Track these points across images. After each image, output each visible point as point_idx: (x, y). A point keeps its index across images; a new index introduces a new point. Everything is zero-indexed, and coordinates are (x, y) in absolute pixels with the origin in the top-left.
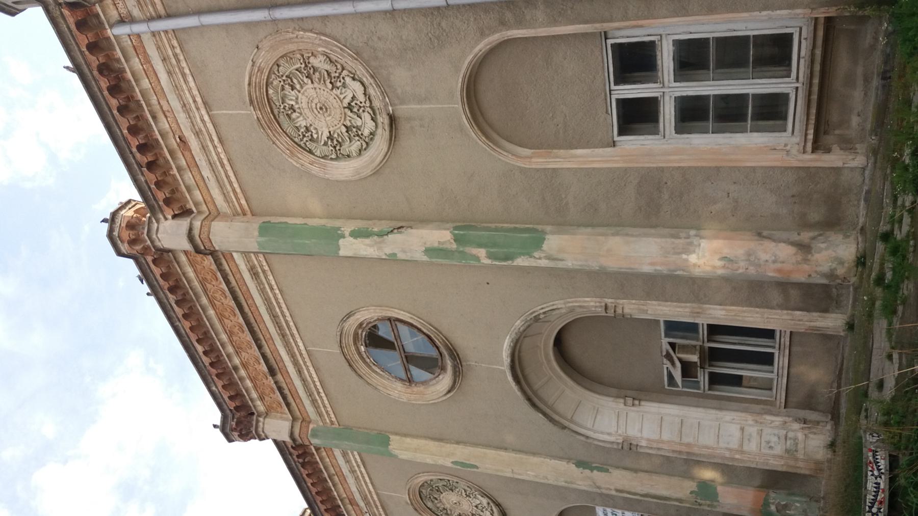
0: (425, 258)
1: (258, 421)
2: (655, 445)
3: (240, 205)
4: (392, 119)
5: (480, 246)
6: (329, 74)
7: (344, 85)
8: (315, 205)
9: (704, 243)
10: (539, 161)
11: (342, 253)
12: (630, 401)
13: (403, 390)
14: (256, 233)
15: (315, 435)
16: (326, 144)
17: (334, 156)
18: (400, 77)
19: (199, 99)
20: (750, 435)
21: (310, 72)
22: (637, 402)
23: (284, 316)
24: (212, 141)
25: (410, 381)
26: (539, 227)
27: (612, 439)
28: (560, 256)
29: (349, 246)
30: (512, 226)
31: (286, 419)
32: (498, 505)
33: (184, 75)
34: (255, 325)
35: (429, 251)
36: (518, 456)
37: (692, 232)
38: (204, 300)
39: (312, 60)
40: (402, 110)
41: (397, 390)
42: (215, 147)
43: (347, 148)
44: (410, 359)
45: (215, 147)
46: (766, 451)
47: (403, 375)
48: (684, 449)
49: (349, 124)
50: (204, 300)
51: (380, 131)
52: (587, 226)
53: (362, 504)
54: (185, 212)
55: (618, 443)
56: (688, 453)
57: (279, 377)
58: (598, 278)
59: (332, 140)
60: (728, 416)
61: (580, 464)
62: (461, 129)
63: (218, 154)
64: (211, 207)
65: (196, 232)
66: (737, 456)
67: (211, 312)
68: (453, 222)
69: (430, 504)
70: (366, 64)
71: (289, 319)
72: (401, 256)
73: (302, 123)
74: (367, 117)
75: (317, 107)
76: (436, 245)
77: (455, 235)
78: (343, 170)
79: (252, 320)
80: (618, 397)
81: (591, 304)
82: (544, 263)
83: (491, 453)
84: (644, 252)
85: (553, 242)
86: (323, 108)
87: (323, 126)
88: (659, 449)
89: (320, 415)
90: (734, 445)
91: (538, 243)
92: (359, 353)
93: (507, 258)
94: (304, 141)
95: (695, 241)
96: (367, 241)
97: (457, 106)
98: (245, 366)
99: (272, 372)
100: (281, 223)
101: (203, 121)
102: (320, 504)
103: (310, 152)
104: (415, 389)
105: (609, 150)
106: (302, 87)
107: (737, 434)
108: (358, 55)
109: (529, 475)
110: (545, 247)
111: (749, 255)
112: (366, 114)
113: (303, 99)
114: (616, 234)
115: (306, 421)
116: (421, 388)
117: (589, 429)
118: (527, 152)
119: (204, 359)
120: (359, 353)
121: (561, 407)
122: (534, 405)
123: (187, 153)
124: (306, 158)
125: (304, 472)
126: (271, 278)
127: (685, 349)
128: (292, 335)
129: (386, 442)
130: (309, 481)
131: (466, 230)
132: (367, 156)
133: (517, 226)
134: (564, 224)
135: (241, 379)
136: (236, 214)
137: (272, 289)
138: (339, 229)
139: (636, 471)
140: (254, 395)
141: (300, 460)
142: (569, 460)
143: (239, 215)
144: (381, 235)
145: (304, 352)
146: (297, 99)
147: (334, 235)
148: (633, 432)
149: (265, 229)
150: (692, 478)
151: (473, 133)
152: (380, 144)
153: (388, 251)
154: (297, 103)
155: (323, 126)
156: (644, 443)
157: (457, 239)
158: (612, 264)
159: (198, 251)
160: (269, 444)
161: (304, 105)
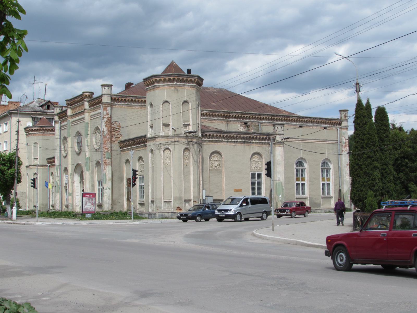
26: (90, 170)
46: (76, 203)
54: (90, 107)
57: (75, 115)
61: (71, 173)
85: (87, 173)
90: (76, 198)
99: (76, 114)
114: (89, 181)
148: (76, 182)
157: (87, 158)
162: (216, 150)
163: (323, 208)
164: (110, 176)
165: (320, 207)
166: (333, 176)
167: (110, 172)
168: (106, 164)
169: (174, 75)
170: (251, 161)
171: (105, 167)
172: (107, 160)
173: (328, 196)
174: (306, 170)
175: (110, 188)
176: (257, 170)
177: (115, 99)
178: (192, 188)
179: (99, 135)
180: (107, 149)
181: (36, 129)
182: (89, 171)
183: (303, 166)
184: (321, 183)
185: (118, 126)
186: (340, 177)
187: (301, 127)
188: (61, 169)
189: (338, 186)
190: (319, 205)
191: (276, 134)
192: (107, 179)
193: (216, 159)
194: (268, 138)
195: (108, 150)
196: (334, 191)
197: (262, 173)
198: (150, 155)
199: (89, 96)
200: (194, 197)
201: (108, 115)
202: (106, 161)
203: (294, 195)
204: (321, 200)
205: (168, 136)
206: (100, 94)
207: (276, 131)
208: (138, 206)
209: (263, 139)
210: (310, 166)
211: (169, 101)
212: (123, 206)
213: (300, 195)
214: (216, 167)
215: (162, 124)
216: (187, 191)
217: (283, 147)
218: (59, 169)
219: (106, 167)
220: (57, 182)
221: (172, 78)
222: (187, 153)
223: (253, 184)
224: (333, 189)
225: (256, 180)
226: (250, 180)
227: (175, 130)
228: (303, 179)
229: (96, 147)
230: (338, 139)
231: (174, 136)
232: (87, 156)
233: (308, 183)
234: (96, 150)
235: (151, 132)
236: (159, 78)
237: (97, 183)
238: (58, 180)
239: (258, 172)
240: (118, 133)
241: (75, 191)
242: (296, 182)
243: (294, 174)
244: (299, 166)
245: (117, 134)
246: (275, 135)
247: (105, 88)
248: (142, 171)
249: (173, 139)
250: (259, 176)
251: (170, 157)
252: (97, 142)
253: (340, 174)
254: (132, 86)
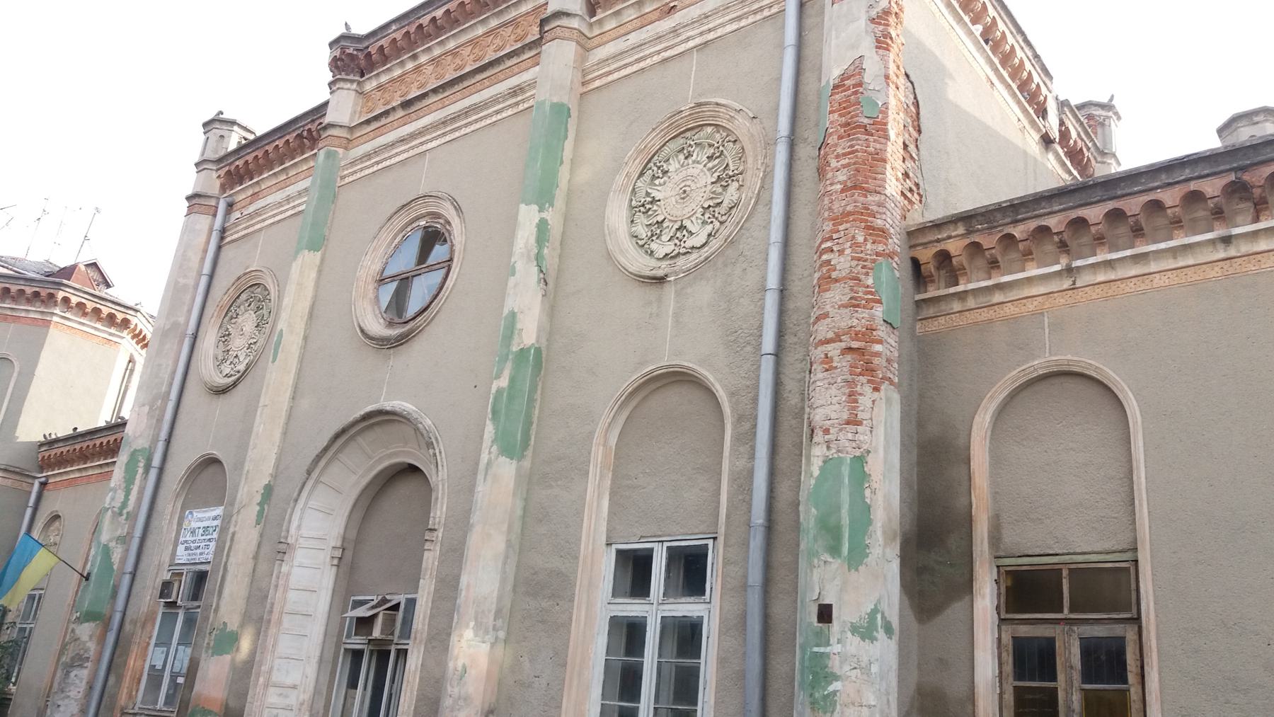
0: (506, 311)
1: (352, 81)
2: (281, 582)
3: (594, 80)
4: (660, 280)
5: (512, 380)
6: (719, 204)
7: (704, 223)
8: (584, 174)
9: (485, 648)
10: (598, 454)
11: (523, 206)
12: (338, 553)
13: (371, 272)
14: (555, 100)
15: (329, 155)
16: (648, 194)
17: (634, 203)
18: (703, 293)
19: (711, 36)
20: (286, 697)
21: (723, 181)
22: (335, 562)
23: (466, 125)
24: (666, 49)
25: (381, 281)
26: (529, 453)
27: (293, 530)
28: (489, 478)
29: (528, 216)
30: (535, 420)
31: (351, 120)
32: (235, 384)
33: (739, 18)
34: (461, 86)
35: (513, 315)
36: (284, 414)
37: (502, 634)
38: (494, 23)
39: (735, 185)
40: (669, 291)
41: (371, 265)
42: (659, 52)
43: (641, 219)
44: (405, 282)
45: (659, 52)
47: (388, 273)
48: (275, 617)
49: (665, 225)
50: (494, 23)
51: (653, 263)
52: (525, 509)
53: (251, 209)
55: (286, 538)
56: (269, 621)
57: (400, 113)
58: (462, 522)
59: (651, 203)
60: (311, 670)
61: (269, 490)
62: (642, 363)
63: (651, 55)
64: (596, 41)
65: (564, 22)
66: (261, 680)
67: (480, 31)
68: (548, 347)
69: (244, 296)
70: (720, 252)
71: (463, 132)
72: (512, 281)
73: (673, 166)
74: (669, 248)
75: (686, 185)
76: (519, 326)
77: (529, 349)
78: (617, 214)
79: (466, 84)
80: (344, 539)
81: (439, 512)
82: (484, 457)
83: (290, 380)
84: (484, 578)
85: (507, 469)
86: (684, 195)
87: (665, 192)
88: (277, 586)
89: (353, 163)
90: (275, 677)
91: (508, 450)
92: (418, 218)
93: (494, 412)
94: (652, 167)
95: (490, 638)
96: (532, 240)
97: (665, 360)
98: (418, 69)
99: (406, 104)
100: (566, 130)
101: (688, 39)
102: (254, 155)
103: (642, 174)
104: (371, 287)
105: (604, 539)
106: (709, 169)
107: (289, 681)
108: (731, 242)
109: (259, 427)
110: (503, 459)
111: (465, 699)
112: (673, 247)
113: (695, 170)
114: (509, 544)
115: (348, 144)
116: (371, 295)
117: (306, 503)
118: (613, 440)
119: (428, 17)
120: (418, 218)
121: (335, 469)
122: (337, 436)
123: (657, 14)
124: (635, 168)
125: (291, 137)
126: (510, 112)
127: (389, 624)
128: (444, 134)
129: (313, 246)
130: (280, 143)
131: (535, 363)
132: (629, 245)
133: (534, 426)
134: (529, 483)
135: (402, 63)
136: (584, 73)
137: (497, 112)
138: (552, 205)
139: (256, 557)
140: (384, 79)
141: (304, 133)
142: (275, 476)
143: (584, 76)
144: (539, 258)
145: (424, 148)
146: (698, 162)
147: (544, 198)
149: (561, 112)
150: (242, 625)
151: (636, 377)
152: (641, 263)
153: (519, 266)
154: (694, 162)
155: (665, 192)
156: (285, 568)
157: (522, 351)
158: (474, 539)
159: (543, 22)
160: (323, 95)
161: (691, 171)
168: (869, 370)
180: (882, 233)
181: (29, 290)
182: (521, 457)
188: (161, 470)
202: (868, 334)
218: (148, 468)
219: (865, 401)
220: (107, 552)
232: (529, 334)
237: (607, 565)
238: (124, 540)
241: (280, 622)
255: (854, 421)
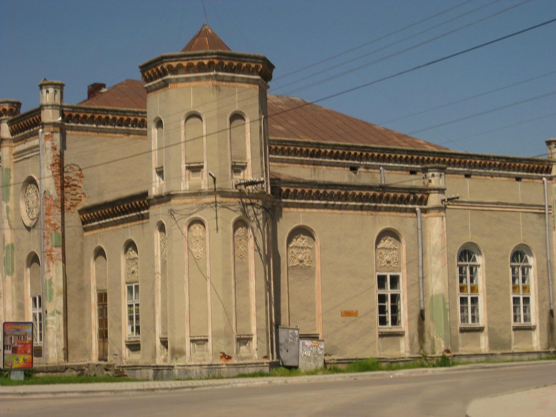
5: (6, 255)
26: (15, 273)
54: (12, 134)
114: (13, 298)
157: (8, 246)
162: (301, 224)
163: (516, 351)
164: (61, 284)
165: (510, 347)
166: (536, 282)
167: (61, 276)
168: (52, 259)
169: (212, 54)
170: (376, 247)
171: (48, 266)
172: (54, 249)
173: (527, 324)
174: (479, 270)
175: (62, 311)
176: (390, 268)
177: (70, 116)
178: (253, 309)
179: (34, 194)
183: (472, 261)
184: (512, 296)
185: (77, 175)
186: (551, 283)
187: (468, 176)
189: (548, 303)
190: (508, 345)
191: (430, 190)
192: (55, 291)
193: (301, 245)
194: (415, 198)
195: (57, 226)
196: (538, 314)
197: (400, 274)
198: (157, 235)
199: (11, 110)
200: (257, 330)
201: (56, 149)
202: (51, 251)
203: (456, 322)
204: (513, 333)
205: (198, 194)
206: (37, 106)
207: (430, 181)
208: (126, 352)
209: (402, 200)
210: (487, 261)
211: (200, 111)
212: (87, 352)
213: (468, 322)
214: (301, 261)
215: (184, 166)
216: (242, 315)
217: (444, 218)
221: (206, 62)
222: (241, 230)
223: (382, 298)
224: (537, 308)
225: (388, 291)
226: (376, 292)
227: (215, 179)
228: (474, 289)
229: (28, 222)
230: (545, 201)
231: (215, 192)
233: (485, 296)
234: (29, 229)
235: (158, 184)
236: (177, 63)
237: (31, 301)
239: (392, 274)
240: (78, 190)
242: (459, 295)
243: (455, 278)
244: (466, 261)
245: (74, 192)
246: (426, 191)
247: (48, 92)
248: (133, 272)
249: (211, 199)
250: (395, 281)
251: (204, 239)
252: (29, 210)
253: (550, 278)
254: (104, 90)
255: (49, 271)
